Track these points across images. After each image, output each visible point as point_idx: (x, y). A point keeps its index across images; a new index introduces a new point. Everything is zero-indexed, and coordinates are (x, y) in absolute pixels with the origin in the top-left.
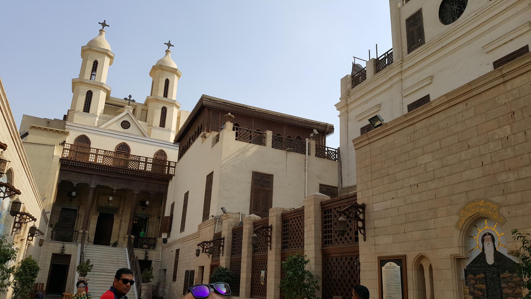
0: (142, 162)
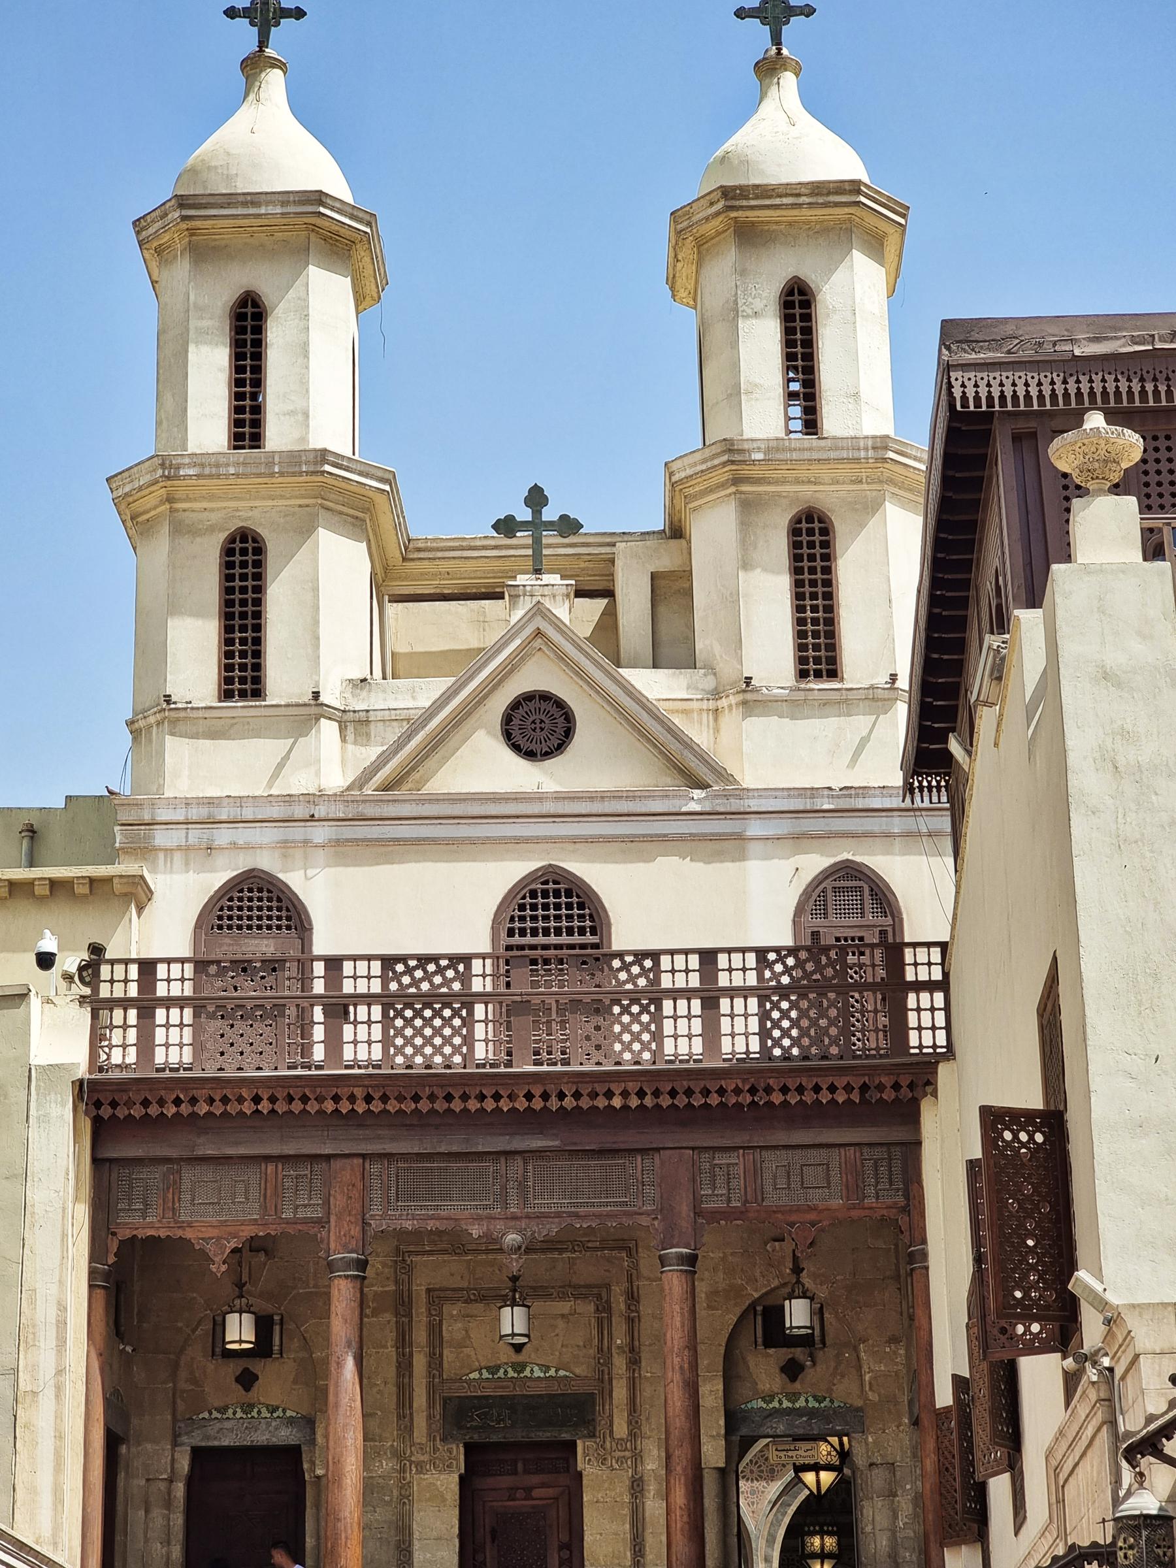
0: (675, 994)
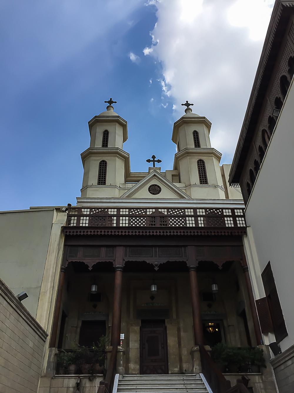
0: (189, 216)
